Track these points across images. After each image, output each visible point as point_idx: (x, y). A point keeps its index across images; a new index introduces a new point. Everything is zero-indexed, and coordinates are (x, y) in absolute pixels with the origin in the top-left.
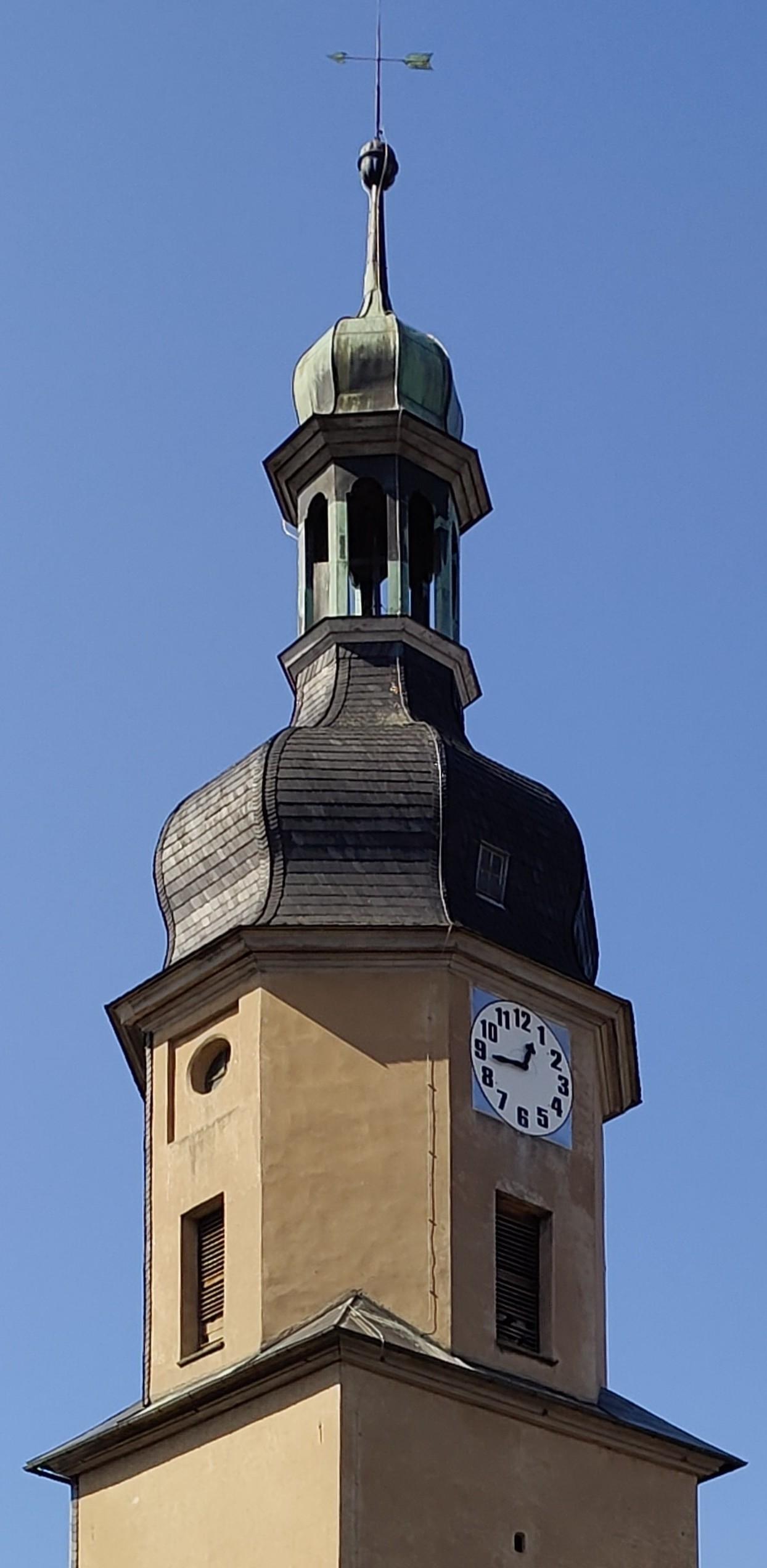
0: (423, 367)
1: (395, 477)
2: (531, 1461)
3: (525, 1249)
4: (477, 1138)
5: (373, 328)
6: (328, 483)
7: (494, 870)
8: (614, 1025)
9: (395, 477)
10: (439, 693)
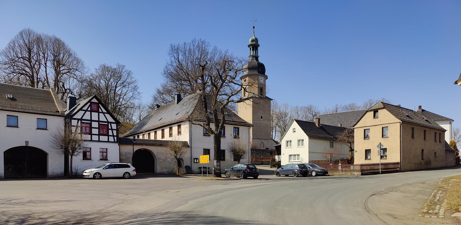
0: (256, 40)
1: (255, 46)
2: (262, 101)
3: (262, 90)
4: (259, 84)
5: (254, 38)
6: (251, 47)
7: (260, 69)
8: (266, 77)
9: (255, 46)
10: (257, 58)
